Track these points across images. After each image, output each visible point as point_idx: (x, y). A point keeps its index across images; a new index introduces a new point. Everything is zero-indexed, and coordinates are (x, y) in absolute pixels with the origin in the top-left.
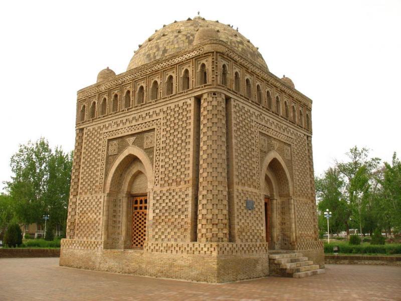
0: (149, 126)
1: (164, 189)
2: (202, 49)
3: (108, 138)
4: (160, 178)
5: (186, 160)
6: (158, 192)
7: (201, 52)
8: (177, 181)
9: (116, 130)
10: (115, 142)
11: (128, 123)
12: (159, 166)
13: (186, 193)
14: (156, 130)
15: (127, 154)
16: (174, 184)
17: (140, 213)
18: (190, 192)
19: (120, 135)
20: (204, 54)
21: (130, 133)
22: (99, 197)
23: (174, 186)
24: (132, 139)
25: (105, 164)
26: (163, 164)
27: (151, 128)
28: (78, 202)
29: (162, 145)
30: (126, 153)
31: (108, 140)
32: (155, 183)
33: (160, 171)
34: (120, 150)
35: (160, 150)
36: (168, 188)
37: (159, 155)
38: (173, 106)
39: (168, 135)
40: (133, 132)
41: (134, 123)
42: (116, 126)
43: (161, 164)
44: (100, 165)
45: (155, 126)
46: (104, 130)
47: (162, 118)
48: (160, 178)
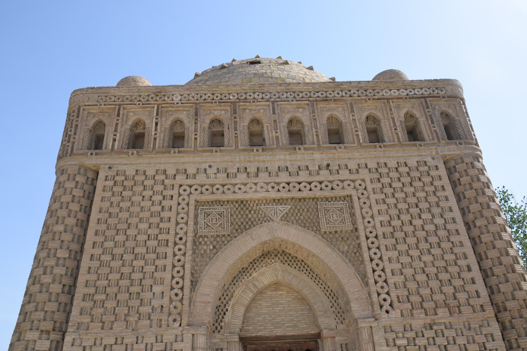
0: (332, 189)
7: (441, 93)
8: (447, 305)
9: (223, 186)
10: (220, 209)
13: (485, 331)
14: (355, 199)
15: (266, 238)
16: (442, 312)
18: (495, 329)
19: (240, 196)
21: (273, 194)
22: (168, 337)
25: (189, 253)
27: (339, 192)
32: (381, 307)
35: (376, 237)
38: (392, 164)
40: (284, 194)
41: (284, 177)
44: (170, 254)
45: (349, 191)
46: (180, 179)
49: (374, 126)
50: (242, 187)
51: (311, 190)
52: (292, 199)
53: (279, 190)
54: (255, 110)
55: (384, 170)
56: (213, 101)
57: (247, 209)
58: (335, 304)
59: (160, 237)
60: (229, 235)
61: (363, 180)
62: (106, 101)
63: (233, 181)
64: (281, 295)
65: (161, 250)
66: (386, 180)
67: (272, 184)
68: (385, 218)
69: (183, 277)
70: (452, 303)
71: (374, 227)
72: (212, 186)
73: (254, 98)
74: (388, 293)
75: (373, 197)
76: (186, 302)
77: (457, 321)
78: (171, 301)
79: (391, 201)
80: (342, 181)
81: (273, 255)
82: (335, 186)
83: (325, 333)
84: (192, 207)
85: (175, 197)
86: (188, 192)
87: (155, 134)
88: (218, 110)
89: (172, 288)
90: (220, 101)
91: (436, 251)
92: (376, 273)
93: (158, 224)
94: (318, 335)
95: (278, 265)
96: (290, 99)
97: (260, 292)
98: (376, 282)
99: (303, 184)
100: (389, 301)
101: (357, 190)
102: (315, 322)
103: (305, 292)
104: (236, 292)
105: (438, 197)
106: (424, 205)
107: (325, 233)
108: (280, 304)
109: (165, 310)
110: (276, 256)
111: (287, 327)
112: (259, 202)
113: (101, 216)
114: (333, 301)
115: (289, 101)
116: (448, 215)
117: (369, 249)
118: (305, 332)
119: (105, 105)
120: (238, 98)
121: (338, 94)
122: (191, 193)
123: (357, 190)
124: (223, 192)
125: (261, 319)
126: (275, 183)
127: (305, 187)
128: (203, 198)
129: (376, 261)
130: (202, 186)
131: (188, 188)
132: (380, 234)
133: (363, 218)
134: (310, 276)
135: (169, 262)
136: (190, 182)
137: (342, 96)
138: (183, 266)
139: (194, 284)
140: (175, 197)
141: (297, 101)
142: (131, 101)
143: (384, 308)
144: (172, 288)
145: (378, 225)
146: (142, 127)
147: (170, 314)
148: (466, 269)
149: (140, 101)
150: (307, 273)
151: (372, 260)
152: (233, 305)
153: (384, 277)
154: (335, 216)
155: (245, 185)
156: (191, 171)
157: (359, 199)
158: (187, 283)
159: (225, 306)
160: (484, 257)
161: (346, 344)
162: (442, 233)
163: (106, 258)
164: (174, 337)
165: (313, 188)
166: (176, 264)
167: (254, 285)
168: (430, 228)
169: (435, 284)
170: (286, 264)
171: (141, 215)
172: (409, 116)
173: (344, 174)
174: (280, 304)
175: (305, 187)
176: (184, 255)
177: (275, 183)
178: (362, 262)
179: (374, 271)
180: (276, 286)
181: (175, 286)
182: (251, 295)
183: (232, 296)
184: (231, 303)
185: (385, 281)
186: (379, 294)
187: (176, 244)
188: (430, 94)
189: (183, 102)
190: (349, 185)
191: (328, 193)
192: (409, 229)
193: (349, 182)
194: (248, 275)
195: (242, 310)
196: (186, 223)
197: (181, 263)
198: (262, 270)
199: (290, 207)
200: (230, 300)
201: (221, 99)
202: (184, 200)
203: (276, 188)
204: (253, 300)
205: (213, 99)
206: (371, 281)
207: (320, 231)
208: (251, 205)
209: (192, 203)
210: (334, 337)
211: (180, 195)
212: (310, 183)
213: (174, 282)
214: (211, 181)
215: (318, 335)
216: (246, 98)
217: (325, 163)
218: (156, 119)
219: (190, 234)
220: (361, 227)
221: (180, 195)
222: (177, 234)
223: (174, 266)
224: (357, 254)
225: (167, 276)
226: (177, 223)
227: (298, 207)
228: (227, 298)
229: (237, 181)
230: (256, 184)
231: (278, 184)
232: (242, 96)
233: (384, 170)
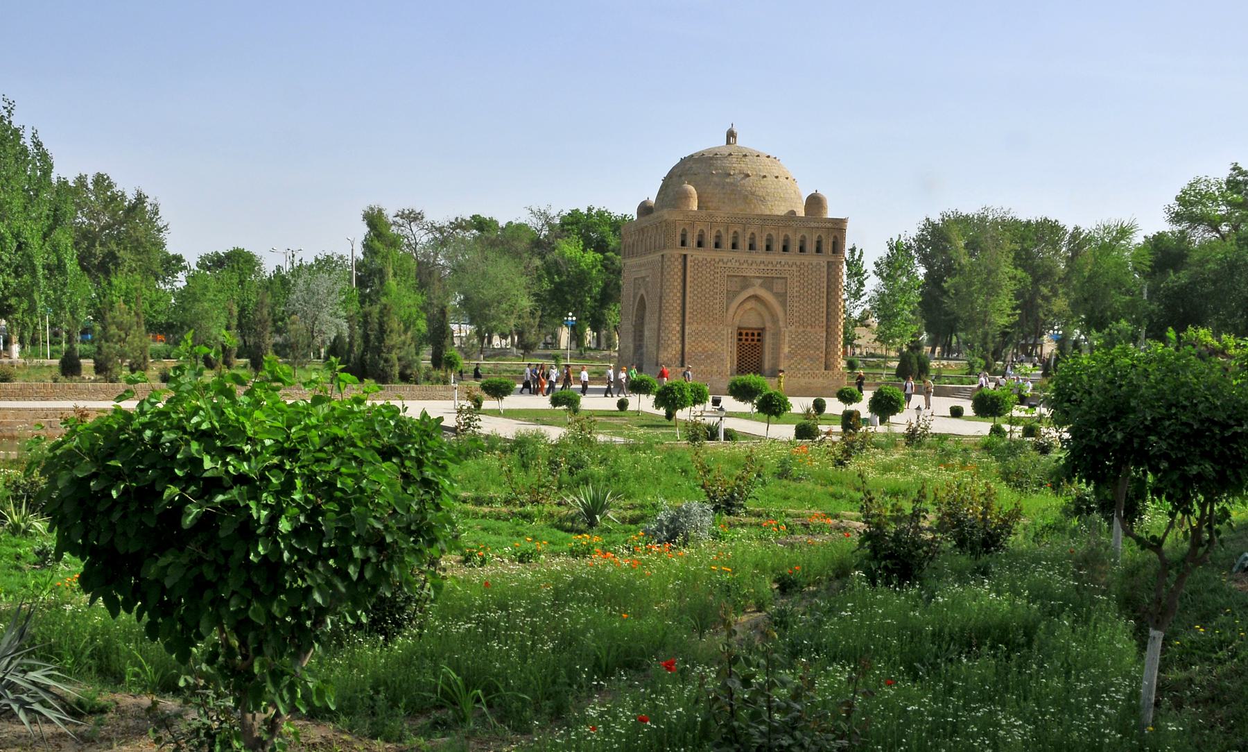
11: (754, 265)
15: (752, 293)
24: (760, 281)
27: (783, 275)
28: (687, 331)
30: (750, 292)
34: (744, 288)
40: (761, 275)
41: (762, 267)
42: (737, 264)
77: (813, 331)
102: (764, 323)
112: (751, 277)
128: (731, 274)
139: (727, 310)
156: (725, 260)
172: (820, 236)
173: (787, 267)
215: (763, 329)
225: (718, 306)
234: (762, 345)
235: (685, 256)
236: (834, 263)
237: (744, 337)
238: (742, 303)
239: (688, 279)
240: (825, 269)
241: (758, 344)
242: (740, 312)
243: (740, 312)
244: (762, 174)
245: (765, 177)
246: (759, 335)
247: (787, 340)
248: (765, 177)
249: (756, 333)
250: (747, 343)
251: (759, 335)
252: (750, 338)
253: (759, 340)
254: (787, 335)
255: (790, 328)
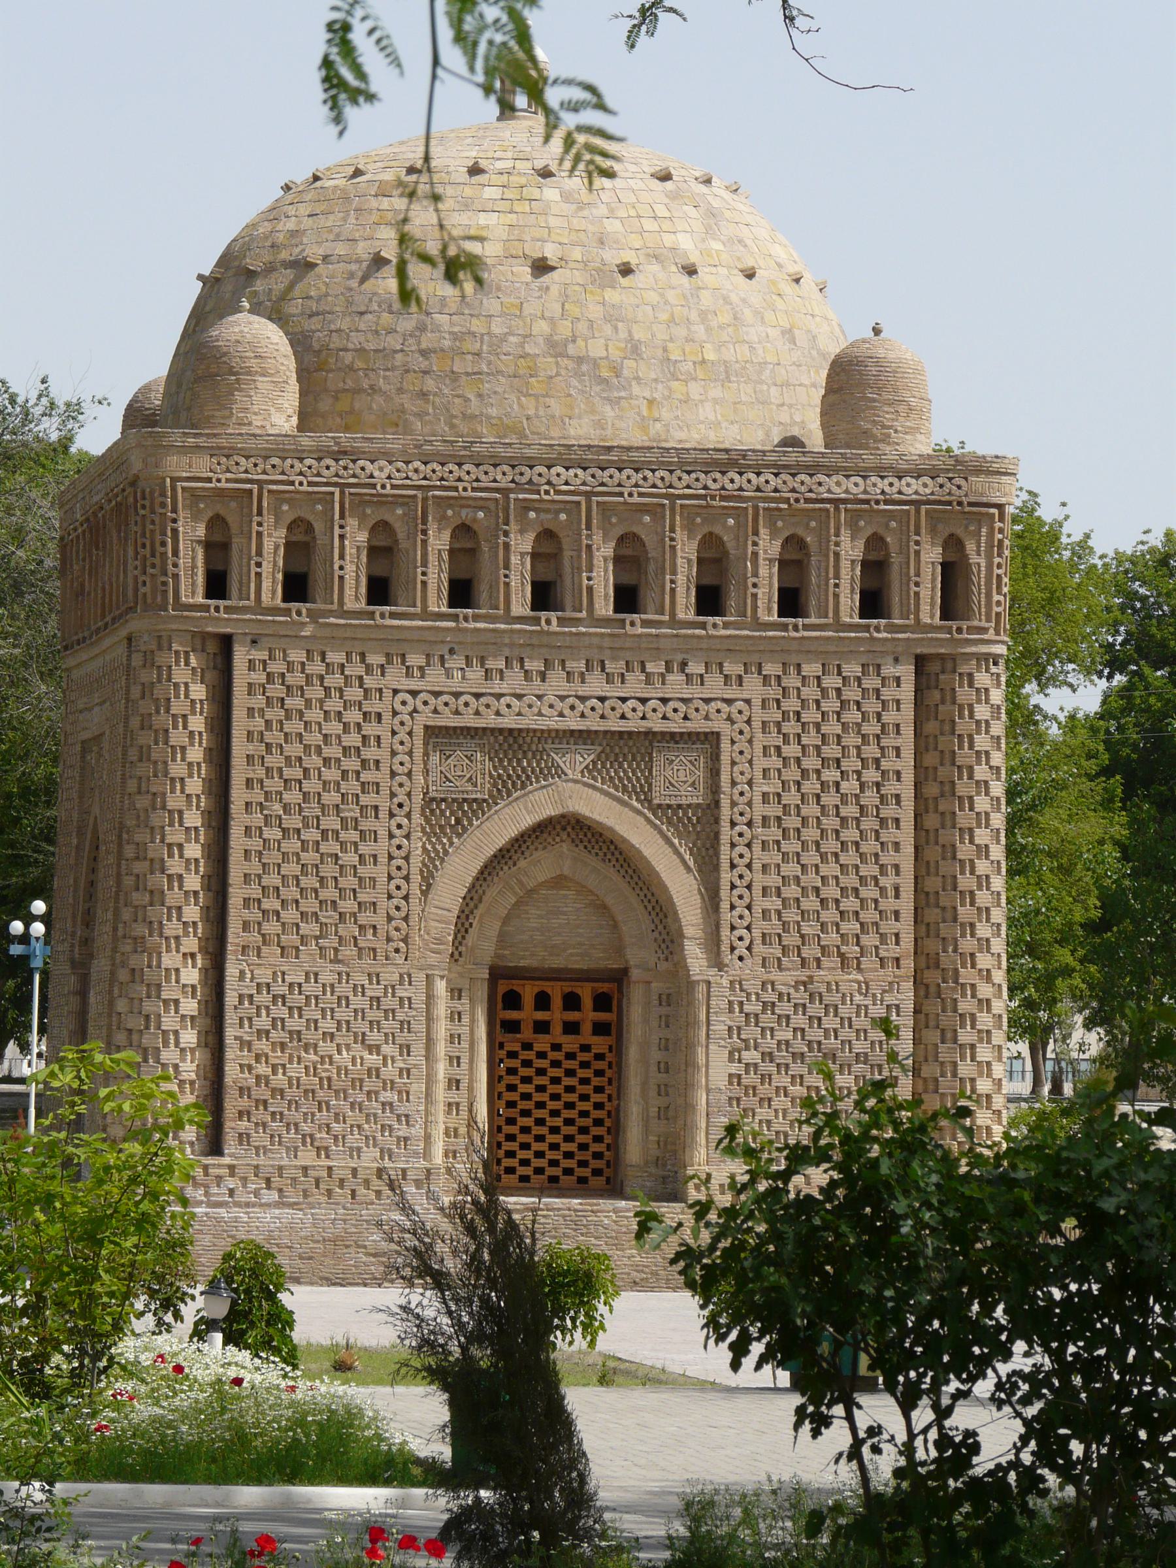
1: (785, 979)
2: (962, 482)
3: (425, 718)
4: (756, 933)
5: (887, 882)
6: (752, 986)
9: (477, 696)
12: (749, 887)
13: (889, 999)
15: (550, 811)
17: (537, 1047)
18: (906, 996)
20: (970, 504)
21: (574, 723)
22: (390, 975)
23: (829, 971)
26: (773, 880)
27: (697, 725)
29: (759, 810)
31: (426, 727)
32: (733, 949)
33: (757, 910)
35: (749, 824)
36: (802, 975)
37: (749, 845)
39: (793, 774)
40: (593, 724)
43: (759, 880)
44: (383, 833)
45: (718, 725)
47: (757, 702)
48: (756, 933)
49: (794, 557)
50: (515, 702)
51: (643, 718)
52: (606, 732)
53: (583, 715)
54: (547, 511)
55: (792, 681)
56: (460, 485)
57: (520, 747)
58: (660, 927)
59: (365, 800)
60: (485, 800)
61: (748, 701)
62: (228, 470)
63: (497, 686)
64: (565, 896)
65: (366, 825)
66: (791, 704)
67: (571, 700)
68: (772, 787)
69: (407, 878)
70: (852, 950)
71: (750, 804)
72: (457, 695)
73: (549, 483)
74: (748, 928)
75: (760, 740)
76: (413, 920)
78: (390, 919)
79: (791, 750)
80: (707, 701)
81: (558, 827)
82: (692, 714)
83: (635, 974)
84: (419, 742)
85: (387, 717)
86: (410, 708)
87: (341, 568)
88: (469, 506)
89: (390, 897)
90: (475, 484)
91: (850, 858)
92: (736, 892)
93: (358, 773)
94: (625, 971)
95: (565, 847)
96: (626, 491)
97: (531, 892)
98: (733, 907)
99: (631, 703)
100: (747, 942)
101: (733, 723)
102: (620, 950)
103: (610, 901)
104: (488, 893)
105: (882, 749)
106: (852, 763)
107: (660, 806)
108: (564, 913)
109: (381, 933)
110: (564, 829)
111: (572, 955)
113: (251, 748)
114: (657, 921)
115: (621, 494)
116: (890, 788)
117: (733, 845)
118: (602, 964)
119: (228, 481)
120: (513, 481)
121: (732, 481)
122: (415, 711)
123: (733, 723)
124: (477, 713)
125: (525, 937)
126: (577, 697)
127: (634, 710)
129: (741, 869)
130: (437, 694)
131: (408, 697)
132: (758, 820)
133: (734, 783)
134: (622, 872)
135: (382, 847)
136: (414, 685)
137: (741, 489)
138: (407, 858)
140: (387, 717)
141: (640, 495)
142: (283, 473)
143: (737, 952)
144: (390, 897)
145: (757, 799)
146: (302, 529)
147: (389, 940)
148: (891, 892)
149: (301, 474)
150: (618, 866)
151: (733, 866)
152: (481, 916)
153: (747, 900)
154: (682, 773)
155: (519, 697)
157: (733, 742)
158: (415, 891)
159: (467, 917)
160: (932, 870)
161: (669, 995)
162: (869, 824)
163: (273, 834)
164: (396, 977)
165: (650, 714)
166: (396, 853)
167: (520, 882)
168: (850, 810)
169: (830, 915)
170: (581, 847)
171: (327, 752)
173: (715, 686)
174: (564, 913)
175: (634, 710)
176: (407, 836)
177: (577, 697)
178: (716, 868)
179: (733, 887)
180: (559, 882)
181: (395, 893)
182: (513, 900)
183: (480, 901)
184: (477, 913)
185: (749, 907)
186: (733, 928)
187: (392, 815)
188: (932, 493)
189: (394, 482)
190: (718, 711)
191: (676, 726)
192: (811, 810)
193: (720, 705)
194: (510, 863)
195: (497, 925)
196: (409, 774)
197: (403, 853)
198: (536, 854)
199: (599, 749)
200: (476, 907)
201: (477, 480)
202: (402, 723)
203: (580, 707)
204: (518, 904)
205: (459, 480)
206: (725, 906)
207: (650, 802)
208: (528, 739)
209: (419, 731)
210: (649, 983)
211: (395, 713)
212: (644, 701)
213: (392, 886)
214: (456, 683)
216: (530, 482)
217: (679, 657)
218: (341, 527)
219: (418, 798)
220: (725, 802)
221: (395, 713)
222: (393, 795)
223: (391, 858)
224: (711, 852)
225: (380, 872)
226: (393, 774)
227: (617, 750)
228: (472, 904)
229: (504, 687)
230: (539, 697)
231: (583, 699)
232: (522, 474)
233: (792, 681)
234: (618, 1048)
235: (226, 643)
236: (949, 662)
237: (527, 1014)
238: (503, 856)
239: (240, 748)
240: (907, 691)
241: (600, 1044)
242: (499, 898)
243: (499, 898)
244: (613, 257)
245: (626, 270)
246: (602, 1002)
247: (719, 1028)
248: (626, 270)
249: (586, 994)
250: (542, 1043)
251: (602, 1002)
252: (557, 1015)
253: (601, 1029)
254: (719, 1002)
255: (736, 969)
